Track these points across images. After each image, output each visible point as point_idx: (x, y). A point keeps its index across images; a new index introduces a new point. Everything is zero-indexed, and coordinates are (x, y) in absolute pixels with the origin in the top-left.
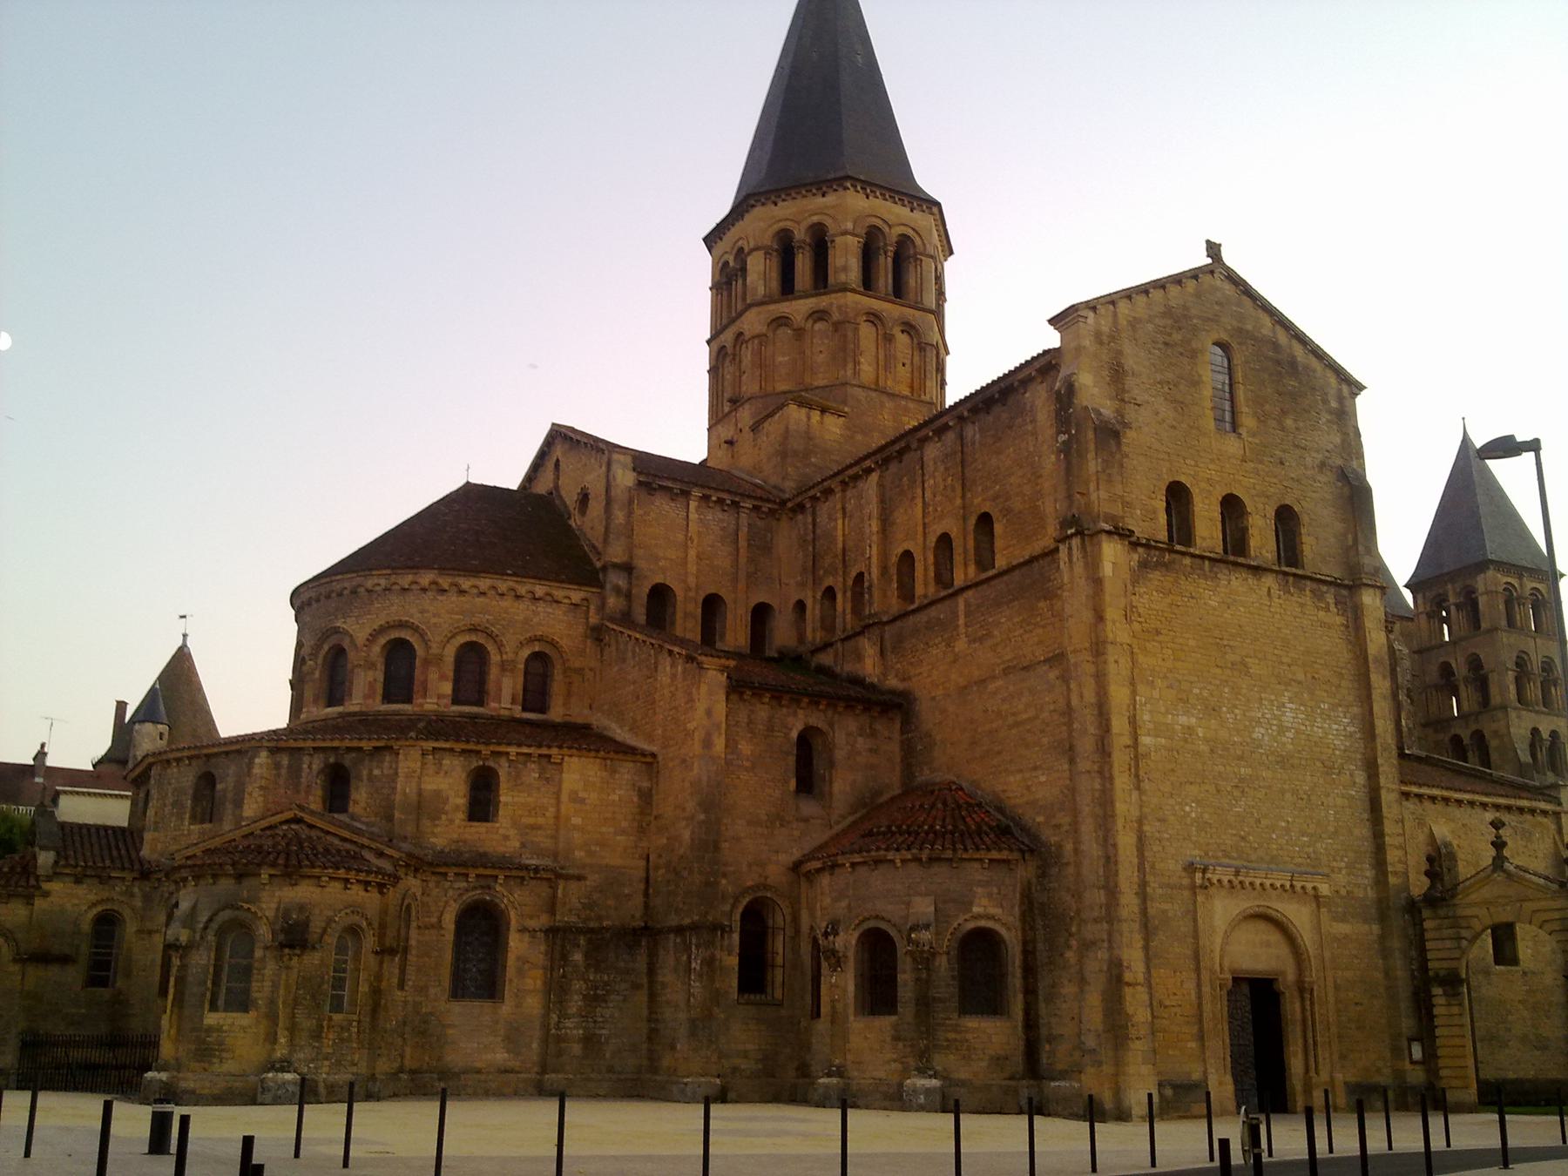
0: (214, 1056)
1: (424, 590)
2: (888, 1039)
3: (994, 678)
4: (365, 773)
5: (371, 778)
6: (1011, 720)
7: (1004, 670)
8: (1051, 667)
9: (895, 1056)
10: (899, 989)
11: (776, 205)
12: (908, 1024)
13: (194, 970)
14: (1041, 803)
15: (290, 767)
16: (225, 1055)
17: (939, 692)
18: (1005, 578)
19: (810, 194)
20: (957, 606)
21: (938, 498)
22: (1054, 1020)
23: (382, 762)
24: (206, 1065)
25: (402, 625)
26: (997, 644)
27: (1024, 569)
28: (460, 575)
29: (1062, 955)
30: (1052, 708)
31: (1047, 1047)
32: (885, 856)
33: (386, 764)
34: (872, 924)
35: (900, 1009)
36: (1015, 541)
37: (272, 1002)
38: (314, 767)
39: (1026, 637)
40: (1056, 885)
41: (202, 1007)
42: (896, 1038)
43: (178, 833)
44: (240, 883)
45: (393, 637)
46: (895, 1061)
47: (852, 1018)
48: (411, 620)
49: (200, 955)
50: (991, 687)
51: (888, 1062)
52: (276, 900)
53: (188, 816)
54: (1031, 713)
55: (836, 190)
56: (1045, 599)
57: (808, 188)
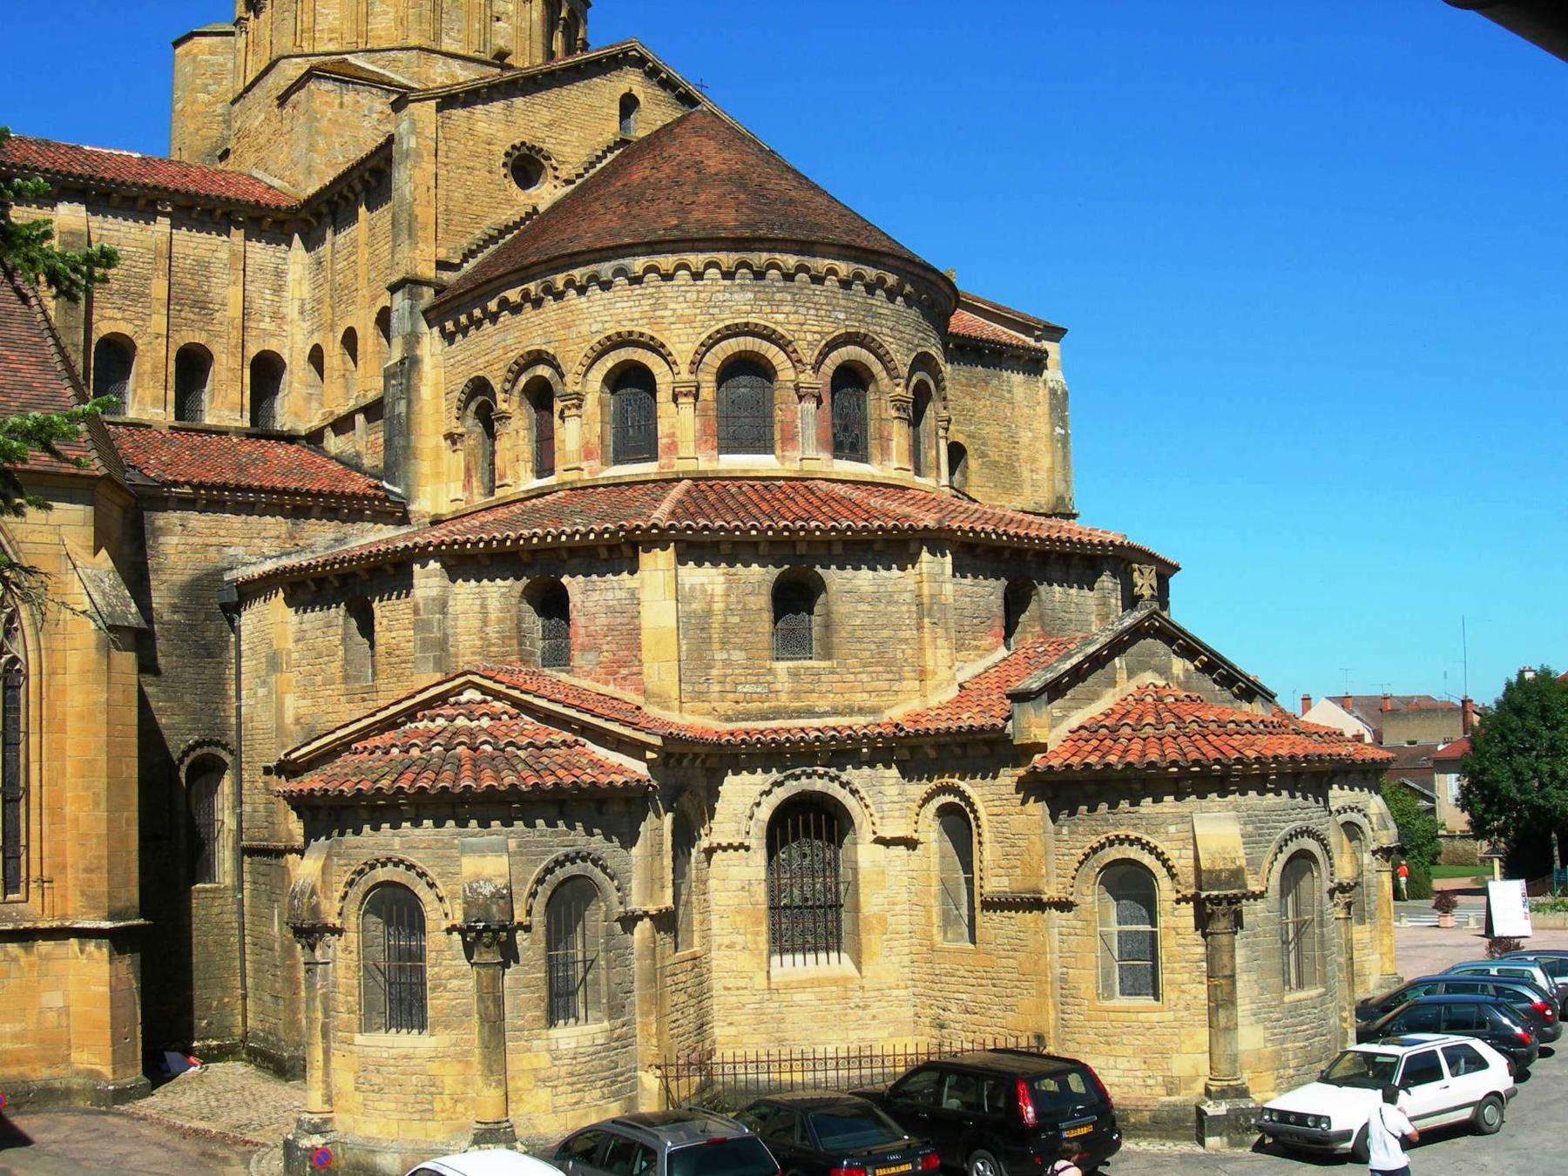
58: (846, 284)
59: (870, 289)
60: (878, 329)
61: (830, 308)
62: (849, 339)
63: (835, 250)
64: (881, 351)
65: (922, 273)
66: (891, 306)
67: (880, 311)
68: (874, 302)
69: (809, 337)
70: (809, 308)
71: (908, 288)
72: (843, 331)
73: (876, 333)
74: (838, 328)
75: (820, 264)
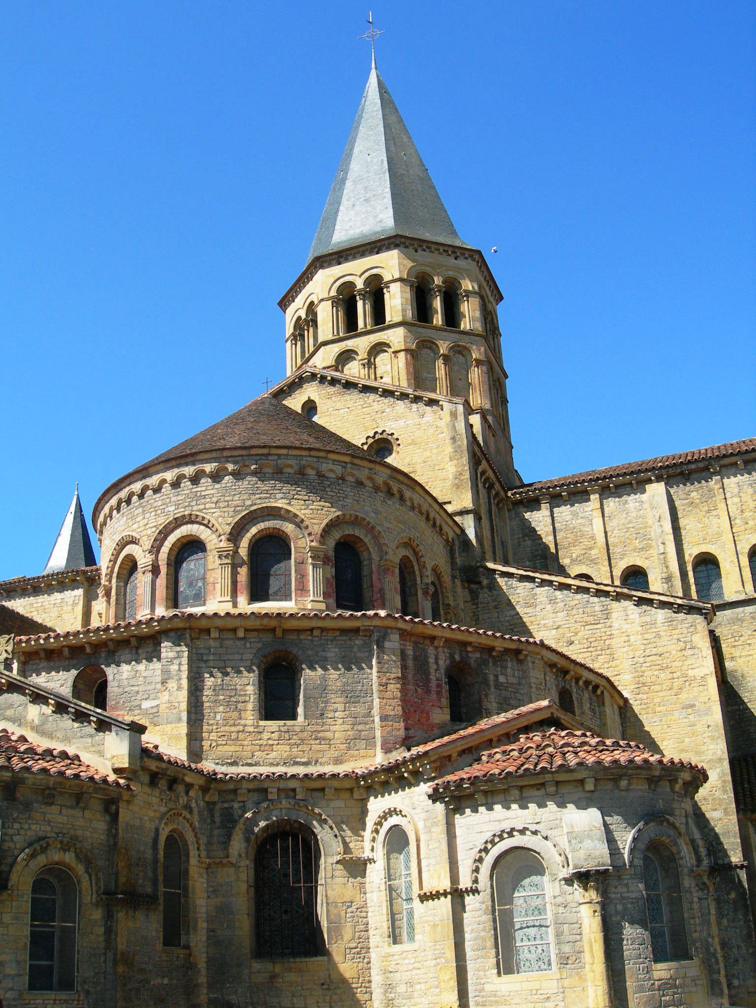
1: (377, 489)
4: (491, 678)
5: (498, 685)
11: (416, 251)
13: (620, 907)
15: (415, 658)
19: (445, 254)
21: (747, 514)
23: (506, 668)
25: (356, 521)
28: (402, 483)
33: (509, 670)
38: (441, 662)
43: (233, 729)
45: (347, 532)
48: (368, 519)
49: (627, 885)
53: (250, 706)
55: (466, 258)
57: (446, 248)
58: (176, 484)
59: (195, 480)
60: (202, 507)
61: (164, 506)
62: (178, 522)
63: (161, 466)
64: (206, 522)
65: (244, 452)
66: (217, 486)
67: (203, 493)
68: (199, 489)
69: (149, 532)
70: (151, 512)
71: (230, 467)
72: (172, 518)
73: (200, 511)
74: (168, 519)
75: (153, 481)
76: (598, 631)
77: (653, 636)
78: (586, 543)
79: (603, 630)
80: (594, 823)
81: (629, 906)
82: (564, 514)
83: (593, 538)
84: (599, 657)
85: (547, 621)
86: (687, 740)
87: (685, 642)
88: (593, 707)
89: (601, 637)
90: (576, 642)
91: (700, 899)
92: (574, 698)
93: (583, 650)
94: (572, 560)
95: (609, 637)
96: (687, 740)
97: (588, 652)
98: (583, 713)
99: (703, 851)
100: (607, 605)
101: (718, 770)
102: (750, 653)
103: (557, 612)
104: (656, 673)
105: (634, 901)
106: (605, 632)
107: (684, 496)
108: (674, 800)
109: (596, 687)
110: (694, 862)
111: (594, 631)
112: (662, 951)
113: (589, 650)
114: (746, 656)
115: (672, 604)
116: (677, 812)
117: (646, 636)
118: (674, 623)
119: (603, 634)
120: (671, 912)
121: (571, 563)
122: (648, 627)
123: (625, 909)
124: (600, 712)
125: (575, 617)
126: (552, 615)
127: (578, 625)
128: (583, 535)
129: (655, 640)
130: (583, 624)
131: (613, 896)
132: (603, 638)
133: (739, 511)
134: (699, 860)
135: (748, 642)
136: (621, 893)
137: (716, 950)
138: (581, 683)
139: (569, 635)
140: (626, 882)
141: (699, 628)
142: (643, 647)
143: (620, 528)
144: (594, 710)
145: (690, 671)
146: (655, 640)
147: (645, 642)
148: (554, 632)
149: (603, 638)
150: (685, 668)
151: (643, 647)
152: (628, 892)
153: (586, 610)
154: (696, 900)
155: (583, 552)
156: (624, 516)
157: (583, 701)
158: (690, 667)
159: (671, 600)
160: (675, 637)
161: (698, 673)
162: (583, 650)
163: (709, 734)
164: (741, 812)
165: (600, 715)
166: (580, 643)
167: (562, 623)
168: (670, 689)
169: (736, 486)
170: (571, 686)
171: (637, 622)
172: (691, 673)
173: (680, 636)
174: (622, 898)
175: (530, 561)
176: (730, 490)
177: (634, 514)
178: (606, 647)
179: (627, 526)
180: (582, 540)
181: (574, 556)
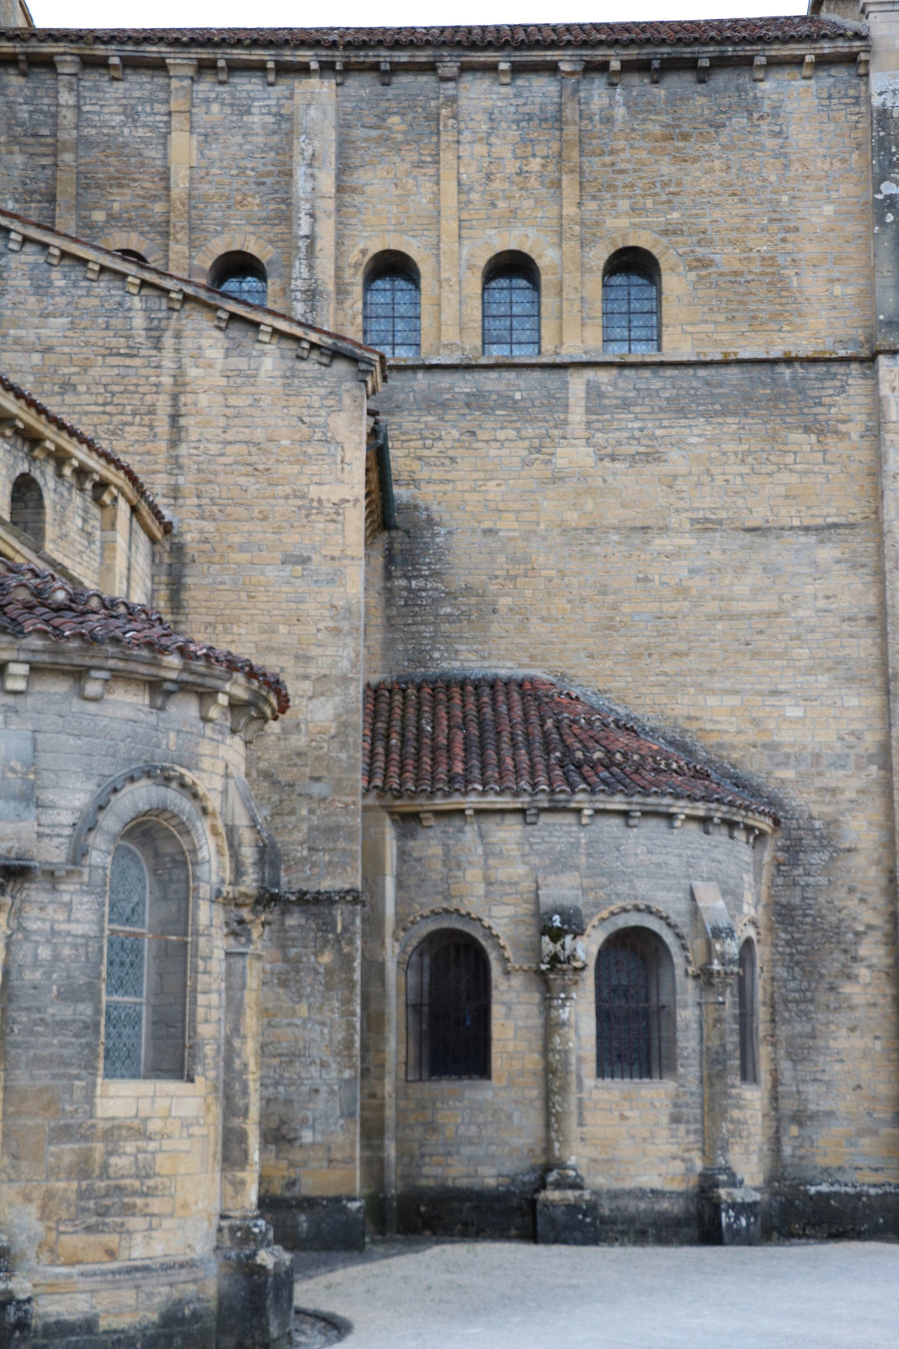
0: (129, 1210)
2: (665, 1120)
3: (664, 529)
6: (713, 607)
7: (693, 521)
8: (821, 542)
9: (675, 1149)
10: (679, 1035)
12: (692, 1094)
13: (44, 953)
14: (787, 750)
16: (156, 1205)
17: (508, 525)
18: (702, 372)
20: (565, 385)
21: (496, 185)
22: (811, 1089)
24: (111, 1240)
26: (675, 477)
27: (756, 372)
29: (832, 989)
30: (822, 604)
31: (794, 1130)
32: (670, 806)
34: (633, 920)
35: (681, 1070)
36: (721, 318)
37: (230, 1054)
39: (755, 480)
40: (823, 880)
41: (91, 1067)
42: (676, 1119)
44: (162, 709)
46: (674, 1158)
47: (590, 1081)
50: (660, 543)
51: (662, 1160)
52: (221, 770)
54: (769, 604)
56: (807, 430)
76: (131, 371)
77: (247, 402)
78: (147, 185)
79: (143, 372)
80: (13, 763)
81: (67, 951)
82: (106, 110)
83: (165, 175)
84: (127, 428)
85: (21, 333)
86: (283, 629)
87: (312, 425)
88: (88, 528)
89: (137, 385)
90: (82, 388)
91: (228, 954)
92: (47, 502)
93: (94, 408)
94: (111, 217)
95: (154, 389)
96: (283, 629)
97: (104, 413)
98: (64, 537)
99: (249, 854)
100: (160, 320)
101: (337, 699)
102: (449, 476)
103: (47, 316)
104: (242, 480)
105: (80, 941)
106: (147, 377)
107: (374, 120)
108: (203, 736)
109: (102, 486)
110: (228, 875)
111: (123, 371)
112: (128, 1057)
113: (108, 409)
114: (442, 482)
115: (298, 339)
116: (206, 763)
117: (233, 400)
118: (296, 381)
119: (142, 381)
120: (160, 975)
121: (107, 222)
122: (239, 381)
123: (56, 957)
124: (103, 543)
125: (88, 333)
126: (36, 321)
127: (88, 352)
128: (143, 164)
129: (248, 410)
130: (103, 351)
131: (33, 926)
132: (141, 389)
133: (482, 175)
134: (238, 871)
135: (451, 453)
136: (53, 922)
137: (246, 1065)
138: (67, 471)
139: (66, 371)
140: (66, 898)
141: (347, 400)
142: (222, 422)
143: (225, 164)
144: (90, 534)
145: (313, 488)
146: (248, 410)
147: (228, 411)
148: (36, 358)
149: (141, 389)
150: (305, 480)
151: (222, 422)
152: (69, 920)
153: (114, 322)
154: (219, 954)
155: (139, 202)
156: (239, 139)
157: (68, 513)
158: (316, 479)
159: (298, 331)
160: (294, 411)
161: (330, 493)
162: (94, 408)
163: (331, 624)
164: (374, 793)
165: (103, 548)
166: (89, 392)
167: (55, 342)
168: (265, 519)
169: (485, 117)
170: (43, 474)
171: (219, 366)
172: (314, 492)
173: (305, 411)
174: (54, 932)
175: (16, 201)
176: (471, 125)
177: (260, 140)
178: (143, 409)
179: (242, 163)
180: (137, 176)
181: (116, 207)
